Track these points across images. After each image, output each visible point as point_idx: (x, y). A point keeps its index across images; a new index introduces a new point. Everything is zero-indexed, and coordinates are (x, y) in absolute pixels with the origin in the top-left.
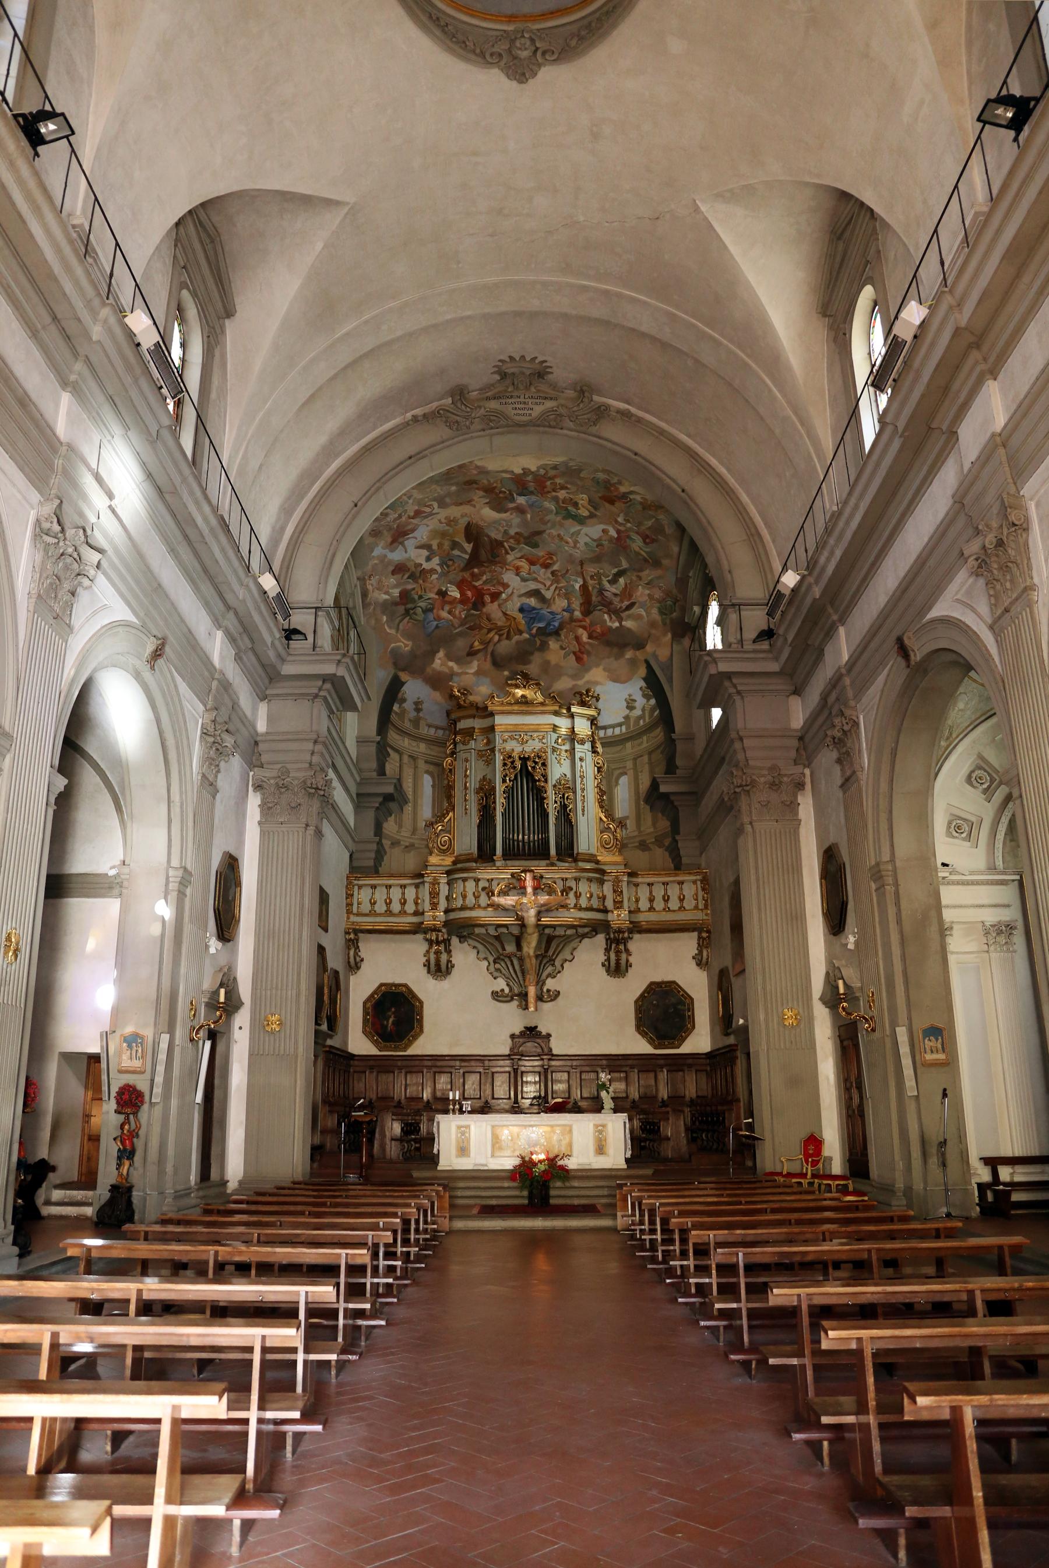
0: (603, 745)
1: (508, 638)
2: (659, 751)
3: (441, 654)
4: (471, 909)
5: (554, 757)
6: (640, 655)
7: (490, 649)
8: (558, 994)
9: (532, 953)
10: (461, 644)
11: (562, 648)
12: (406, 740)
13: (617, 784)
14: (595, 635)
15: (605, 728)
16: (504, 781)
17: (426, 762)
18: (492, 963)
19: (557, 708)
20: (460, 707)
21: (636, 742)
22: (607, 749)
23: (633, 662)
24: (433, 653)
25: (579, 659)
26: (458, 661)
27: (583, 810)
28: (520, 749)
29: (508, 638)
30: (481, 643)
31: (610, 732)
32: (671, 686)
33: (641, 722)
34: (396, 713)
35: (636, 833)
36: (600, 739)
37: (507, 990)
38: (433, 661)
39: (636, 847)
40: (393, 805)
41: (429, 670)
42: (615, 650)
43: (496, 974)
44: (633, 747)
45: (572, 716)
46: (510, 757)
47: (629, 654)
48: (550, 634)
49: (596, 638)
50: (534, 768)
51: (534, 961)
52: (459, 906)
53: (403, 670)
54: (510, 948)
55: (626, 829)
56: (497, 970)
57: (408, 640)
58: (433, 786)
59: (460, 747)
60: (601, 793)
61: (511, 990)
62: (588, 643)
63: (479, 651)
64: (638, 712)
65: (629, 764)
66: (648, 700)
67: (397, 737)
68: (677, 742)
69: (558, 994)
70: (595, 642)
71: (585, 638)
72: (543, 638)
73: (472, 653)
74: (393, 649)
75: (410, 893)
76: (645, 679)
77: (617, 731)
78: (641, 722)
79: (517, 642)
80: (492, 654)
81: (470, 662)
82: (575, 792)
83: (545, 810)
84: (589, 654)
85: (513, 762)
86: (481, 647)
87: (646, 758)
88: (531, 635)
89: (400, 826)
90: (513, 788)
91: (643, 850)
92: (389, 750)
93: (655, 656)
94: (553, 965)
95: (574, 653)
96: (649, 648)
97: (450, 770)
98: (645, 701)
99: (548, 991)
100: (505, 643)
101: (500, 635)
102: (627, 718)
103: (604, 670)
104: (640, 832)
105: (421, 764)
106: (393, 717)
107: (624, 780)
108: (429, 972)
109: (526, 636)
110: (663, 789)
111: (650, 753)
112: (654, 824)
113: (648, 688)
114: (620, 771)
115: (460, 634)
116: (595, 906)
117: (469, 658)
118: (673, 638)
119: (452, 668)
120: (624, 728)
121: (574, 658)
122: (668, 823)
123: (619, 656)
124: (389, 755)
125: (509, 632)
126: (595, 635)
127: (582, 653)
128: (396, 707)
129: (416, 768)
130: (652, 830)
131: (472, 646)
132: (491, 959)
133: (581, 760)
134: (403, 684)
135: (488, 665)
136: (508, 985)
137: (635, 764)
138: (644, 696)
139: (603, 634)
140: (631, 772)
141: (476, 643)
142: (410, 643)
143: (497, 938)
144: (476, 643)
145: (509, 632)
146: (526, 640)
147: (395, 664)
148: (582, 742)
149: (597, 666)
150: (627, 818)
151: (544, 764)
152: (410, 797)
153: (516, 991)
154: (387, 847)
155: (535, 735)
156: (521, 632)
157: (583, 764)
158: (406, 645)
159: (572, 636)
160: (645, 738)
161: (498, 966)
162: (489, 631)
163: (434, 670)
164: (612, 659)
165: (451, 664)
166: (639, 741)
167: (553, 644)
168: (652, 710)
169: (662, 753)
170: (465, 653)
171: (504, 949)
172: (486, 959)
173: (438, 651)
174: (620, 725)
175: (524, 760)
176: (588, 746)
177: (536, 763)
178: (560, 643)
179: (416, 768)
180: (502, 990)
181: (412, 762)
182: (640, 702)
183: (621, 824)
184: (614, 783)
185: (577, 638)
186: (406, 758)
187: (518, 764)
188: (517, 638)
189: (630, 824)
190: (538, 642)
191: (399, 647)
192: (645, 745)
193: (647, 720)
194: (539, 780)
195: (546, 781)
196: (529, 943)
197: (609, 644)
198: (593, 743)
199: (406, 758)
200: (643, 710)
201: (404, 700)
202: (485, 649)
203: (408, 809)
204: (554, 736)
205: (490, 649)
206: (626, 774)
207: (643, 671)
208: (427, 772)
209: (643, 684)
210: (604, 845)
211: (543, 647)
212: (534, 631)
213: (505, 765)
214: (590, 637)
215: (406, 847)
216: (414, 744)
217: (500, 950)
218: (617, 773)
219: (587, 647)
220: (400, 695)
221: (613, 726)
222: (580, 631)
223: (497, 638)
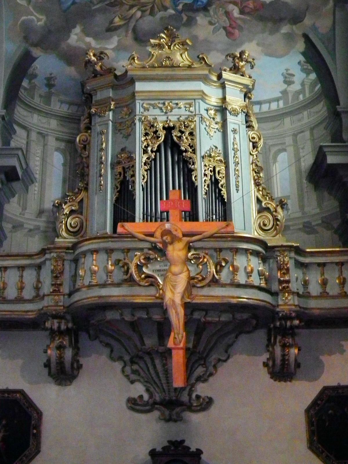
0: (259, 121)
1: (152, 13)
2: (324, 124)
3: (78, 30)
4: (104, 285)
5: (203, 126)
6: (298, 30)
7: (132, 25)
8: (210, 402)
9: (178, 300)
10: (100, 20)
11: (211, 23)
12: (35, 116)
13: (275, 160)
14: (247, 10)
15: (259, 103)
16: (145, 152)
17: (57, 139)
18: (129, 363)
19: (206, 72)
20: (96, 74)
21: (295, 118)
22: (263, 125)
23: (290, 37)
24: (67, 30)
25: (229, 34)
26: (96, 36)
27: (237, 186)
28: (164, 118)
29: (152, 13)
30: (123, 18)
31: (265, 107)
32: (334, 59)
33: (301, 97)
34: (25, 89)
35: (299, 215)
36: (254, 114)
37: (146, 397)
38: (69, 37)
39: (300, 229)
40: (16, 185)
41: (63, 45)
42: (270, 25)
43: (133, 377)
44: (292, 122)
45: (223, 87)
46: (153, 126)
47: (285, 29)
48: (197, 10)
49: (248, 14)
50: (180, 138)
51: (181, 311)
52: (86, 283)
53: (36, 45)
54: (150, 342)
55: (287, 210)
56: (134, 372)
57: (42, 15)
58: (64, 165)
59: (96, 120)
60: (258, 170)
61: (151, 396)
62: (239, 19)
63: (119, 27)
64: (296, 87)
65: (289, 140)
66: (308, 73)
67: (25, 113)
68: (343, 116)
69: (210, 402)
70: (248, 18)
71: (236, 12)
72: (190, 14)
73: (111, 29)
74: (23, 22)
75: (30, 276)
76: (304, 54)
77: (274, 106)
78: (301, 97)
79: (162, 18)
80: (134, 30)
81: (111, 37)
82: (227, 168)
83: (193, 183)
84: (241, 29)
85: (156, 132)
86: (122, 23)
87: (307, 134)
88: (175, 10)
89: (24, 208)
90: (155, 160)
91: (309, 233)
92: (16, 127)
93: (314, 28)
94: (204, 365)
95: (225, 28)
96: (308, 21)
97: (85, 148)
98: (304, 75)
99: (198, 397)
100: (148, 19)
101: (143, 12)
102: (285, 93)
103: (258, 44)
104: (304, 213)
105: (52, 142)
106: (22, 93)
107: (283, 157)
108: (50, 374)
109: (171, 11)
110: (331, 159)
111: (312, 129)
112: (320, 205)
113: (307, 62)
114: (280, 147)
115: (99, 10)
116: (256, 283)
117: (108, 33)
118: (335, 6)
119: (89, 44)
120: (281, 103)
121: (224, 32)
122: (336, 204)
123: (273, 31)
124: (15, 132)
125: (152, 9)
126: (247, 10)
127: (233, 28)
128: (25, 83)
129: (45, 145)
130: (318, 211)
131: (112, 22)
132: (127, 358)
133: (234, 131)
134: (34, 59)
135: (129, 40)
136: (148, 390)
137: (295, 141)
138: (303, 70)
139: (256, 10)
140: (291, 149)
141: (117, 19)
142: (43, 18)
143: (134, 325)
144: (117, 19)
145: (152, 9)
146: (171, 16)
147: (26, 38)
148: (235, 114)
149: (250, 41)
150: (288, 197)
151: (191, 134)
152: (37, 176)
153: (158, 397)
154: (7, 231)
155: (182, 104)
156: (165, 9)
157: (237, 136)
158: (39, 20)
159: (221, 11)
160: (305, 113)
161: (135, 367)
162: (132, 7)
163: (69, 46)
164: (266, 35)
165: (88, 39)
166: (300, 116)
167: (201, 19)
168: (313, 85)
169: (325, 128)
170: (104, 29)
171: (143, 343)
172: (120, 358)
173: (74, 27)
174: (277, 100)
175: (169, 130)
176: (241, 118)
177: (182, 132)
178: (209, 19)
179: (45, 145)
180: (141, 397)
181: (41, 139)
182: (299, 76)
183: (282, 204)
184: (271, 161)
185: (228, 14)
186: (34, 136)
187: (162, 134)
188: (160, 14)
189: (292, 204)
190: (185, 18)
191: (32, 21)
192: (306, 121)
193: (307, 95)
194: (186, 151)
195: (194, 152)
196: (174, 287)
197: (262, 19)
198: (247, 115)
199: (34, 136)
200: (303, 84)
201: (35, 76)
202: (127, 25)
203: (35, 188)
204: (203, 106)
205: (132, 25)
206: (284, 150)
207: (301, 46)
208: (57, 149)
209: (302, 58)
210: (262, 228)
211: (191, 22)
212: (180, 7)
213: (146, 134)
214: (242, 12)
215: (30, 230)
216: (44, 120)
217: (138, 344)
218: (274, 150)
219: (239, 22)
220: (30, 71)
221: (269, 101)
222: (231, 7)
223: (139, 14)
